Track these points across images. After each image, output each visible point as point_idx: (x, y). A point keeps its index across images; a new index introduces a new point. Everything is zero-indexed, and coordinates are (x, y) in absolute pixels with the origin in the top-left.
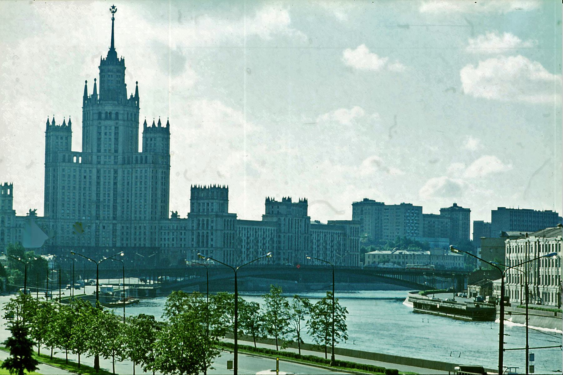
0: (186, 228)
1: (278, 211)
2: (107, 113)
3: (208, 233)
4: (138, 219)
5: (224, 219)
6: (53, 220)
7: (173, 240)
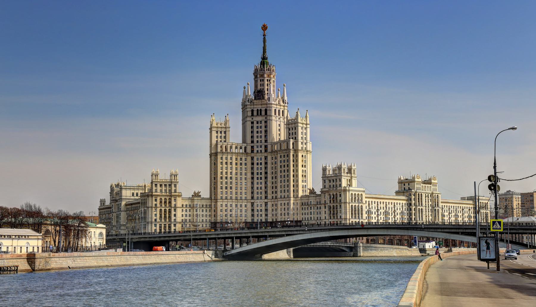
0: (321, 203)
1: (409, 188)
3: (337, 205)
4: (283, 197)
5: (350, 193)
7: (311, 214)
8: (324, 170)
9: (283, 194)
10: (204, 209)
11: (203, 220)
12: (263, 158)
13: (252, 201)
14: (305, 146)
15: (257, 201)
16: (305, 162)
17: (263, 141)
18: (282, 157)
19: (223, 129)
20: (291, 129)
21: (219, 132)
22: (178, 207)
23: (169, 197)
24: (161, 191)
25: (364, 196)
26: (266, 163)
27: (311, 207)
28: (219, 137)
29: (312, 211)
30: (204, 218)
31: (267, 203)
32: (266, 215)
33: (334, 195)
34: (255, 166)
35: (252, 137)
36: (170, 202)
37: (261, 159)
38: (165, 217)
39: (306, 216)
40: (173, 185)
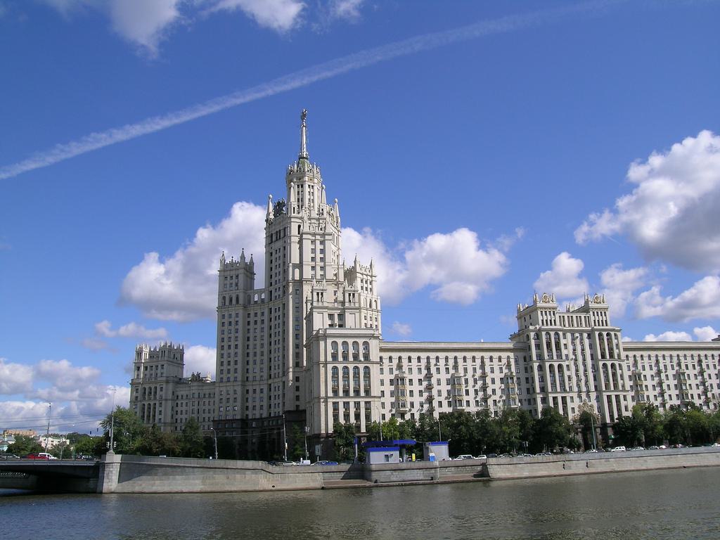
11: (204, 418)
12: (281, 306)
13: (270, 382)
21: (229, 278)
25: (374, 345)
30: (207, 416)
36: (156, 392)
38: (149, 416)
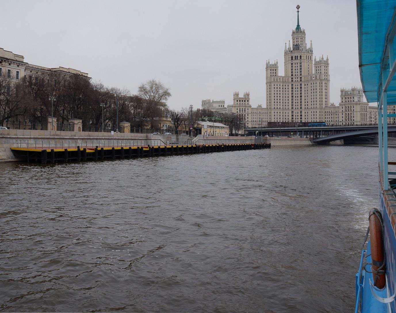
2: (295, 56)
4: (313, 107)
5: (360, 105)
6: (270, 110)
7: (332, 118)
8: (342, 91)
9: (313, 106)
10: (264, 115)
13: (292, 110)
14: (326, 77)
15: (296, 110)
16: (327, 87)
17: (299, 75)
18: (312, 84)
19: (274, 68)
20: (317, 67)
21: (272, 70)
22: (250, 113)
23: (245, 108)
24: (240, 103)
26: (301, 88)
27: (332, 114)
28: (272, 73)
29: (333, 116)
31: (302, 111)
32: (301, 118)
33: (349, 107)
34: (294, 89)
35: (292, 72)
37: (298, 86)
39: (328, 119)
40: (247, 101)
